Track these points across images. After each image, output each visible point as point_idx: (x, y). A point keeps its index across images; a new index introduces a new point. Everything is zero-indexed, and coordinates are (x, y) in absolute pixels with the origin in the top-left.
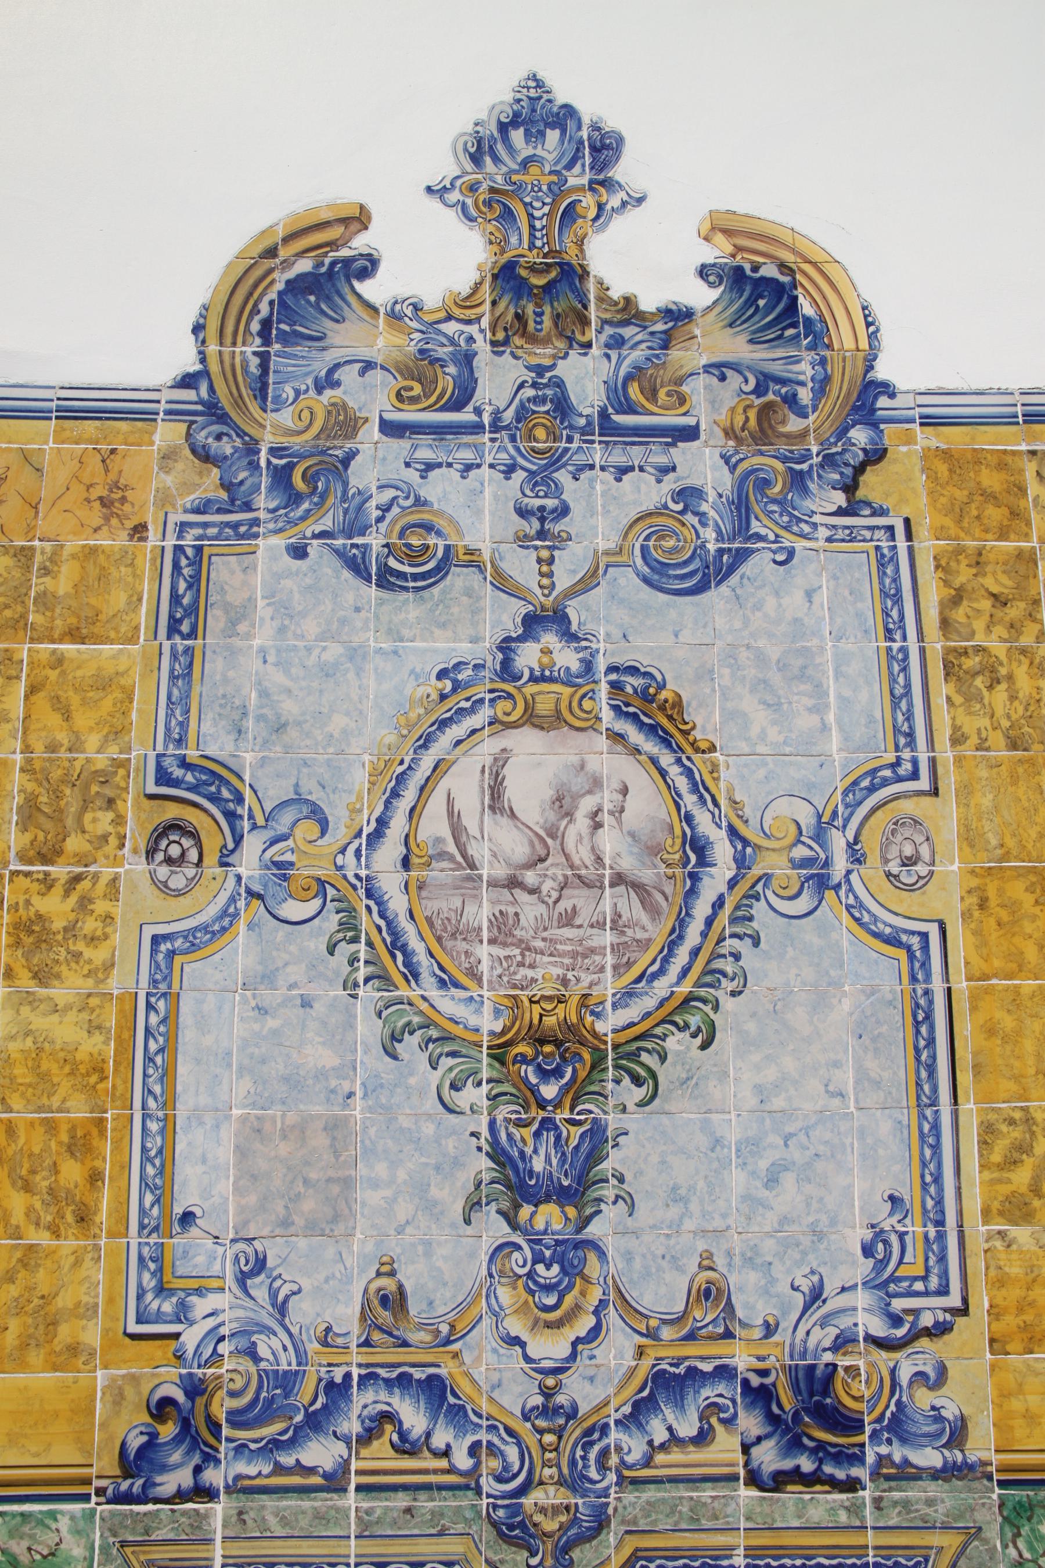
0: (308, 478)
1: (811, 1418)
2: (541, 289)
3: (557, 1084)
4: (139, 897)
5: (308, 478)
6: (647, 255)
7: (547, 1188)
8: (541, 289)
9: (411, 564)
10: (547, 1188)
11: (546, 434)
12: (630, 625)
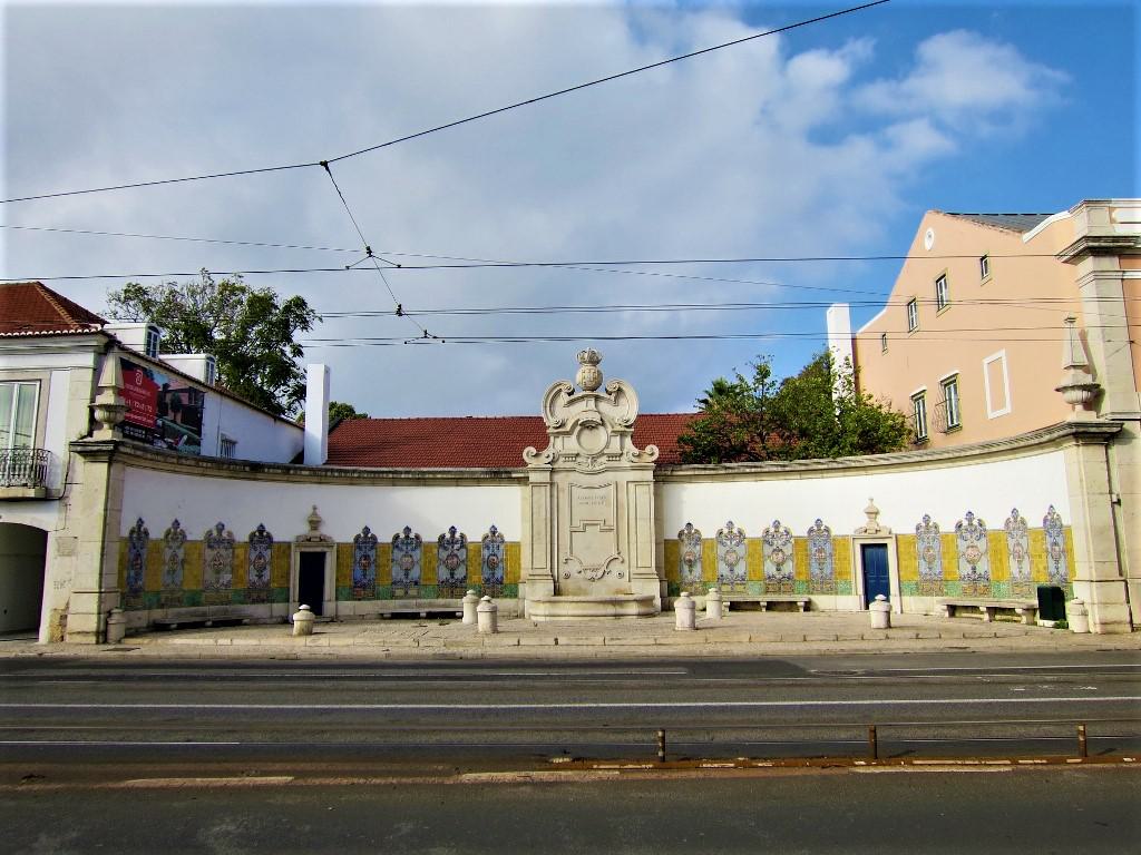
0: (397, 547)
1: (416, 583)
2: (407, 537)
3: (407, 571)
4: (391, 564)
5: (397, 547)
6: (412, 535)
7: (407, 575)
8: (407, 537)
9: (401, 550)
10: (407, 575)
11: (407, 544)
12: (410, 553)
